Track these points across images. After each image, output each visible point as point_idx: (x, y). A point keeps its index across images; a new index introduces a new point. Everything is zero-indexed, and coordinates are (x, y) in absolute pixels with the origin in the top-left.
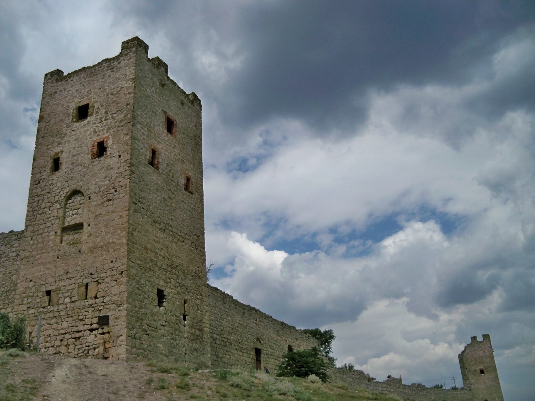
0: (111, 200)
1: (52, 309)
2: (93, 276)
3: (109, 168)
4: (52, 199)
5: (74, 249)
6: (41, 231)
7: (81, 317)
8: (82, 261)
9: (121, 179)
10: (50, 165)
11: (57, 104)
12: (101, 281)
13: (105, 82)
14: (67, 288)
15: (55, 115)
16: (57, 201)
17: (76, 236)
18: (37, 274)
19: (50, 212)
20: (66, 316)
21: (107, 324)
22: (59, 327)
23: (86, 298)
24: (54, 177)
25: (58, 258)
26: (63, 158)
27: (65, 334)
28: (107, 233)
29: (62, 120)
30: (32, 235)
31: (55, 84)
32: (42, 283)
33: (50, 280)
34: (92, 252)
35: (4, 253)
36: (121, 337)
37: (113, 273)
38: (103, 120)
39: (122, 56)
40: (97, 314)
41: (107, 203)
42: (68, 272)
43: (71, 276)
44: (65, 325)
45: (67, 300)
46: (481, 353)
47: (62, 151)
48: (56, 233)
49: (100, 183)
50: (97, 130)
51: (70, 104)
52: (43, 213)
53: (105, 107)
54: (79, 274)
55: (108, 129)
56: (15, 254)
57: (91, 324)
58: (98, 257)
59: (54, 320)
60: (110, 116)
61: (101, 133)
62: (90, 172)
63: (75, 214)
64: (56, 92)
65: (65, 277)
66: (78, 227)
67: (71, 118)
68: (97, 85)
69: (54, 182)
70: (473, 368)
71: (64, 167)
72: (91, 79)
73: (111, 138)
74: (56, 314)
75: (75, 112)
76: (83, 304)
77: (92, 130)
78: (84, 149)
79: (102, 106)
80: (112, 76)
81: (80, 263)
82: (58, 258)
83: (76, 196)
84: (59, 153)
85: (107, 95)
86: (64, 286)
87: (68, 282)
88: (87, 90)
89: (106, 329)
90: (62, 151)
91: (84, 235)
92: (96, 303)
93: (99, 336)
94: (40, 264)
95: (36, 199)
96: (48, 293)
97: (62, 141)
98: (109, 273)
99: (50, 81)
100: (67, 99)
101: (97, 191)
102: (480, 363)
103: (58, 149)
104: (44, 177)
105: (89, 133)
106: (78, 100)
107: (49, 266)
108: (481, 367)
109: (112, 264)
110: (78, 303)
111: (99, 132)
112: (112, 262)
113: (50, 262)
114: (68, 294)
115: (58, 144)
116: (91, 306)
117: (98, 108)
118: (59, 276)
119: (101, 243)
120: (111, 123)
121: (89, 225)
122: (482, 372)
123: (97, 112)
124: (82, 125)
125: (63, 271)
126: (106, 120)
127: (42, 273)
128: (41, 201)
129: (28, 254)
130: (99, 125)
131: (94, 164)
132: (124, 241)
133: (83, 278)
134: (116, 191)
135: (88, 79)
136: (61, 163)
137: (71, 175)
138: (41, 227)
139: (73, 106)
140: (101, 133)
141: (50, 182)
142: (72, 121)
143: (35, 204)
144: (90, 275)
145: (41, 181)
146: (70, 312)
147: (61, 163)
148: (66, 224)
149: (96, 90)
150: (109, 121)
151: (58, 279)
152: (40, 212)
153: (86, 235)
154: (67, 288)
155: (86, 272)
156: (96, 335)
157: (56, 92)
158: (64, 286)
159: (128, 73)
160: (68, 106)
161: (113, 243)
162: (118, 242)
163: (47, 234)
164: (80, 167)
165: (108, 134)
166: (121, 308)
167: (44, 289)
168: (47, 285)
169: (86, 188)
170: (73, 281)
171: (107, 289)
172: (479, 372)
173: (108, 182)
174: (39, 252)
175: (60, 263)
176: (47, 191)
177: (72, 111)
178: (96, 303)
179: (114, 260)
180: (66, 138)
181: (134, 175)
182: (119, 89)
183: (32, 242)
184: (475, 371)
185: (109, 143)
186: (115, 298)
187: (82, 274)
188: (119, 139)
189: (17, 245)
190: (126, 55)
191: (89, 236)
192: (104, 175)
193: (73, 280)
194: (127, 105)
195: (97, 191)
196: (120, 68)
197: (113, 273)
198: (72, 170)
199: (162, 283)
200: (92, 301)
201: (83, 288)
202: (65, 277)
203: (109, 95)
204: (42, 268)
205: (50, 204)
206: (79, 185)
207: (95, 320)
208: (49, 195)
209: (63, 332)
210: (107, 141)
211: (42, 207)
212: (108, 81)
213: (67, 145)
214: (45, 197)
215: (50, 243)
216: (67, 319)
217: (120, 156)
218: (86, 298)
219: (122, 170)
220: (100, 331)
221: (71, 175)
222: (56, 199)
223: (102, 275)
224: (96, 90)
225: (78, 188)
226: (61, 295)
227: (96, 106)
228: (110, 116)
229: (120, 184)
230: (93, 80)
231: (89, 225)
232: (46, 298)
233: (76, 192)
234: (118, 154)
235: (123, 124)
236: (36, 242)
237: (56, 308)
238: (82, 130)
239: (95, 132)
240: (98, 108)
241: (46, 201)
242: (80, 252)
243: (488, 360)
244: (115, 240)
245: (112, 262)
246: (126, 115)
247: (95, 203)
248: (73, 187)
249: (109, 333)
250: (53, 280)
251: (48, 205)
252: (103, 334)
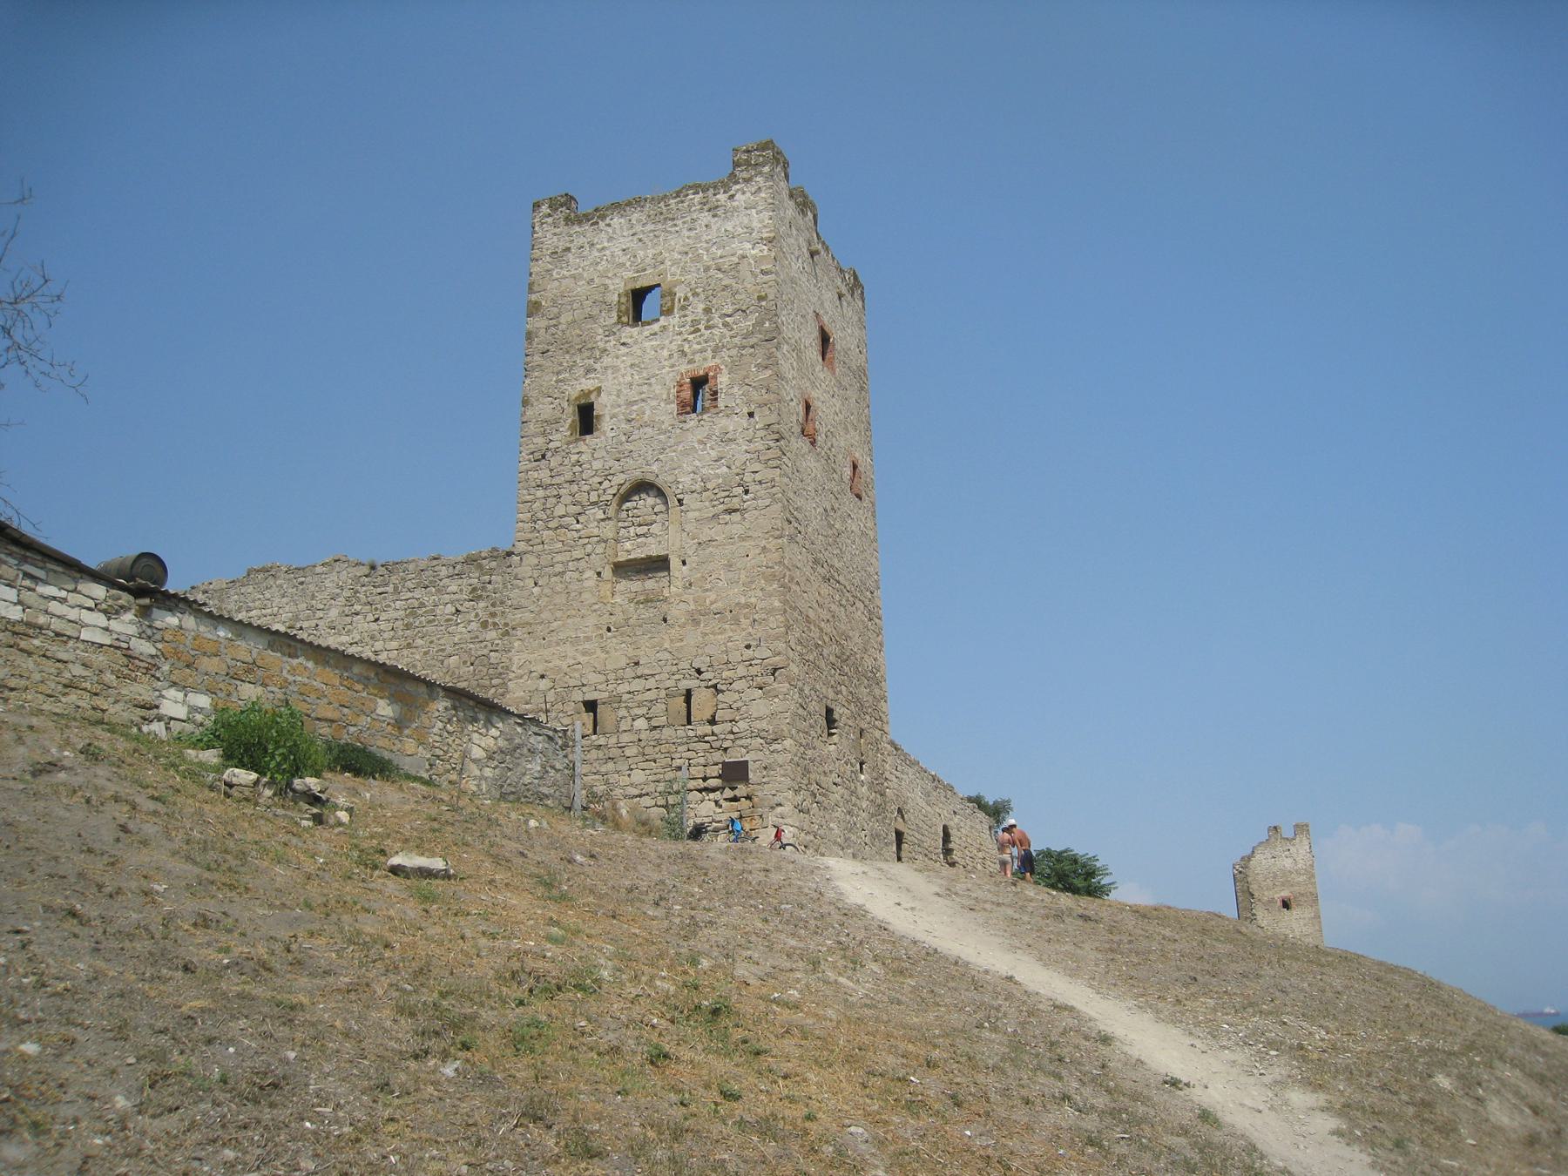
0: (735, 511)
1: (602, 741)
2: (705, 676)
3: (726, 439)
4: (583, 498)
5: (647, 613)
6: (559, 568)
7: (677, 762)
9: (757, 467)
10: (570, 417)
11: (573, 276)
12: (724, 688)
13: (698, 238)
14: (639, 698)
15: (571, 303)
16: (594, 504)
17: (650, 584)
18: (558, 662)
19: (578, 526)
20: (641, 758)
21: (744, 778)
22: (625, 780)
23: (689, 723)
24: (582, 447)
25: (609, 630)
26: (603, 405)
27: (640, 796)
28: (731, 582)
29: (591, 316)
31: (562, 229)
32: (572, 682)
33: (593, 678)
34: (696, 622)
35: (422, 605)
36: (779, 809)
37: (753, 671)
38: (701, 327)
39: (737, 183)
40: (718, 756)
41: (727, 517)
42: (637, 664)
43: (647, 672)
44: (638, 776)
45: (641, 724)
46: (1288, 863)
47: (599, 390)
48: (599, 574)
49: (704, 471)
50: (686, 348)
51: (608, 281)
52: (562, 526)
53: (702, 296)
54: (668, 668)
55: (716, 350)
56: (450, 609)
57: (705, 779)
58: (713, 633)
59: (610, 765)
60: (717, 321)
61: (697, 357)
62: (677, 444)
64: (568, 249)
65: (629, 673)
66: (658, 564)
67: (614, 314)
68: (676, 243)
69: (584, 458)
70: (1267, 895)
71: (607, 425)
72: (660, 226)
73: (725, 371)
74: (615, 752)
75: (623, 300)
76: (681, 733)
77: (674, 347)
78: (657, 389)
79: (695, 294)
80: (714, 227)
81: (666, 645)
83: (643, 496)
84: (590, 392)
85: (707, 269)
87: (637, 685)
88: (651, 252)
89: (742, 790)
90: (599, 390)
91: (672, 585)
92: (713, 734)
93: (725, 804)
95: (540, 493)
96: (591, 706)
97: (597, 366)
98: (742, 670)
99: (550, 220)
100: (600, 268)
101: (698, 487)
102: (1283, 884)
103: (588, 384)
104: (558, 444)
105: (666, 353)
106: (630, 274)
107: (587, 646)
108: (1285, 894)
109: (750, 652)
110: (667, 732)
111: (694, 353)
112: (748, 647)
113: (588, 639)
114: (643, 711)
115: (588, 371)
116: (701, 739)
117: (686, 299)
118: (615, 671)
119: (720, 604)
120: (723, 336)
121: (684, 563)
122: (1286, 905)
123: (683, 308)
124: (646, 333)
125: (623, 662)
126: (707, 328)
128: (554, 500)
129: (528, 616)
130: (691, 337)
131: (686, 426)
132: (777, 604)
134: (747, 492)
135: (652, 227)
136: (598, 417)
137: (629, 447)
138: (559, 558)
139: (618, 287)
140: (697, 357)
141: (574, 458)
142: (619, 321)
143: (537, 505)
145: (549, 454)
146: (647, 751)
147: (598, 417)
148: (622, 557)
149: (676, 256)
150: (715, 331)
151: (612, 676)
152: (552, 525)
153: (679, 583)
154: (639, 698)
155: (685, 665)
156: (716, 802)
157: (568, 249)
159: (756, 224)
160: (606, 287)
161: (747, 606)
162: (763, 604)
163: (576, 575)
164: (649, 430)
165: (717, 361)
166: (775, 746)
167: (578, 696)
169: (670, 479)
170: (651, 683)
171: (740, 704)
172: (1279, 903)
173: (725, 469)
174: (558, 614)
176: (569, 476)
177: (616, 298)
178: (713, 734)
179: (753, 643)
180: (607, 361)
181: (785, 459)
182: (735, 259)
183: (536, 590)
184: (1272, 901)
185: (723, 380)
186: (759, 725)
187: (674, 668)
188: (746, 377)
189: (454, 588)
190: (747, 181)
192: (714, 454)
193: (652, 680)
194: (760, 298)
195: (698, 487)
196: (735, 209)
197: (753, 671)
198: (628, 435)
199: (831, 695)
200: (708, 729)
201: (680, 702)
202: (629, 673)
203: (712, 272)
204: (568, 649)
205: (578, 509)
206: (653, 471)
207: (715, 770)
208: (575, 488)
209: (636, 792)
210: (715, 377)
211: (557, 513)
212: (705, 237)
213: (610, 377)
214: (562, 491)
215: (586, 596)
216: (644, 765)
217: (751, 415)
218: (689, 723)
219: (759, 445)
220: (728, 793)
221: (629, 447)
222: (594, 497)
224: (676, 256)
225: (650, 478)
226: (623, 712)
227: (680, 293)
228: (717, 321)
229: (758, 477)
230: (665, 231)
231: (684, 563)
232: (588, 718)
233: (643, 487)
234: (746, 410)
235: (753, 341)
237: (613, 740)
238: (647, 344)
239: (683, 354)
240: (686, 299)
241: (567, 499)
242: (665, 620)
243: (1301, 879)
244: (753, 600)
245: (748, 647)
246: (760, 323)
247: (697, 514)
248: (637, 475)
249: (748, 798)
250: (602, 678)
251: (573, 509)
252: (735, 799)
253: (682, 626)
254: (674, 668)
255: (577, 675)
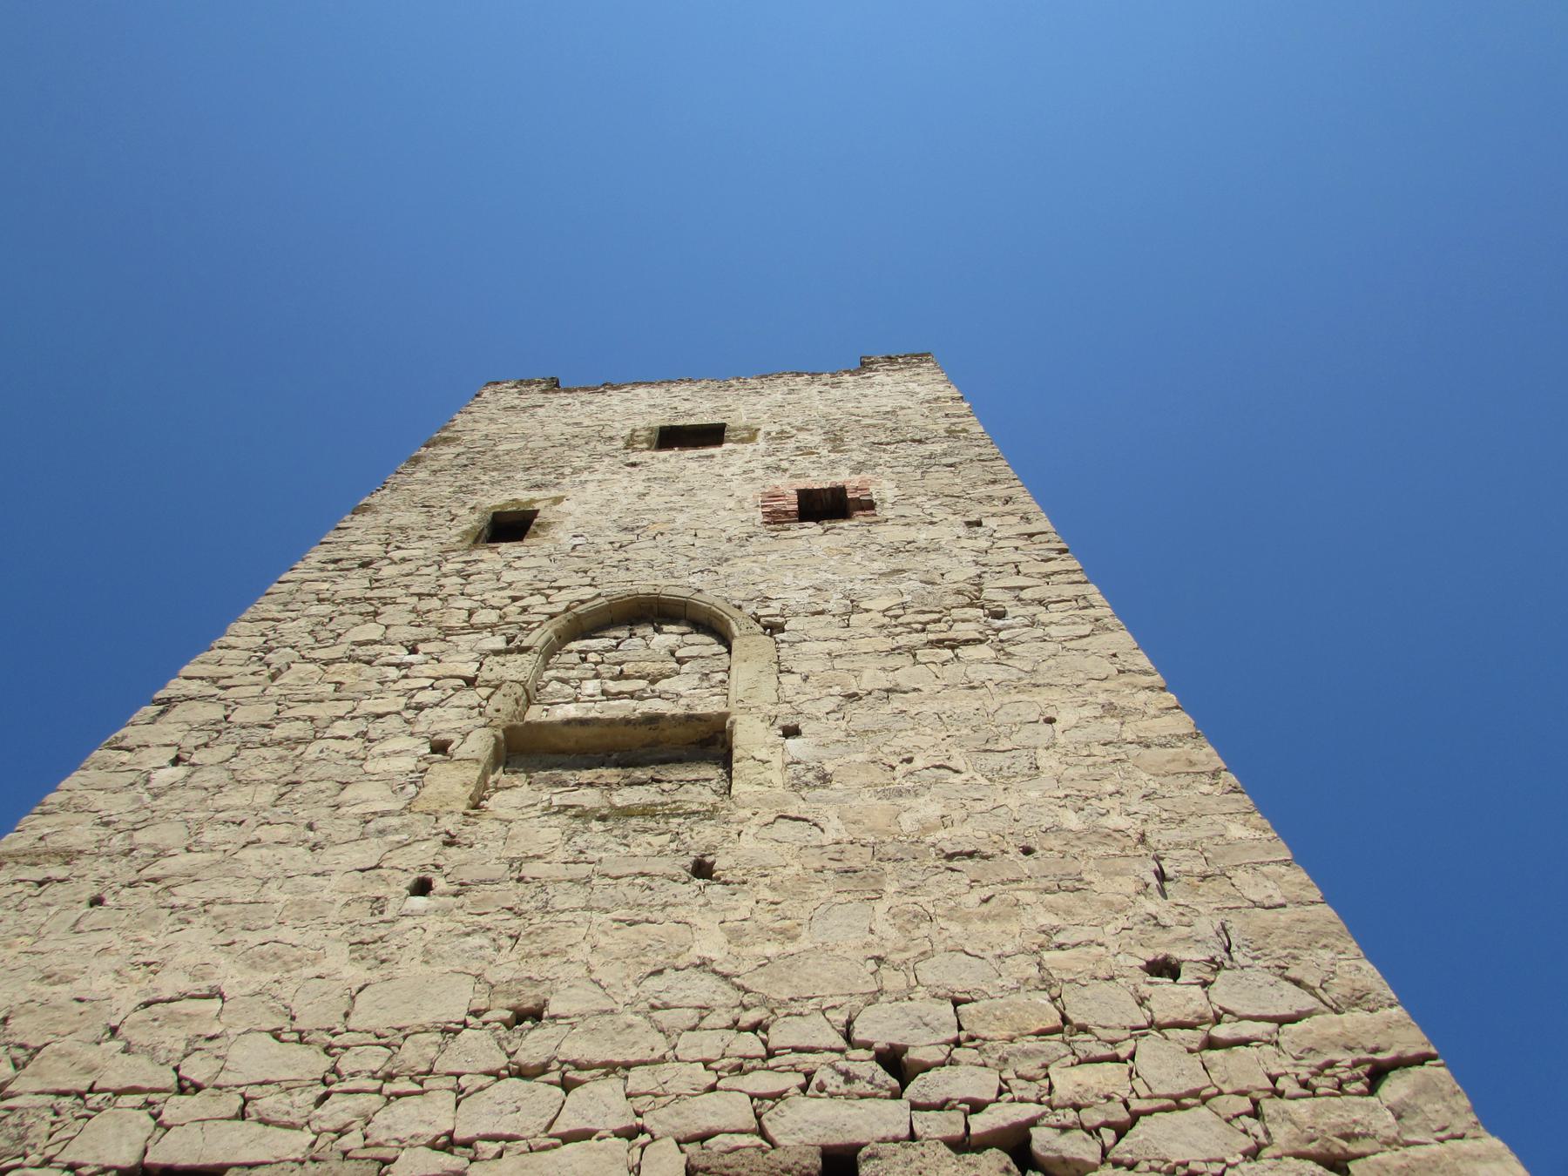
8: (735, 936)
18: (100, 984)
24: (484, 554)
30: (191, 742)
33: (254, 1058)
41: (948, 653)
43: (579, 1048)
54: (709, 1043)
63: (632, 695)
65: (479, 1049)
81: (711, 945)
82: (422, 887)
86: (449, 1143)
94: (183, 915)
107: (288, 934)
109: (1172, 999)
112: (1165, 969)
118: (387, 1041)
127: (169, 984)
133: (762, 1082)
144: (865, 1066)
158: (449, 1143)
168: (175, 1108)
170: (601, 1103)
175: (434, 924)
191: (796, 786)
223: (1067, 1082)
236: (210, 777)
242: (702, 869)
253: (799, 889)
254: (750, 1044)
255: (173, 1039)
